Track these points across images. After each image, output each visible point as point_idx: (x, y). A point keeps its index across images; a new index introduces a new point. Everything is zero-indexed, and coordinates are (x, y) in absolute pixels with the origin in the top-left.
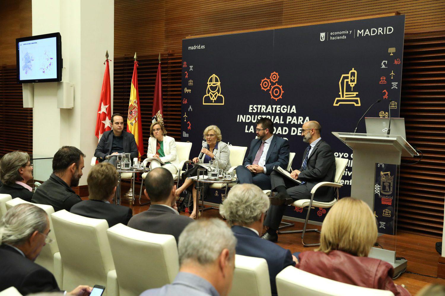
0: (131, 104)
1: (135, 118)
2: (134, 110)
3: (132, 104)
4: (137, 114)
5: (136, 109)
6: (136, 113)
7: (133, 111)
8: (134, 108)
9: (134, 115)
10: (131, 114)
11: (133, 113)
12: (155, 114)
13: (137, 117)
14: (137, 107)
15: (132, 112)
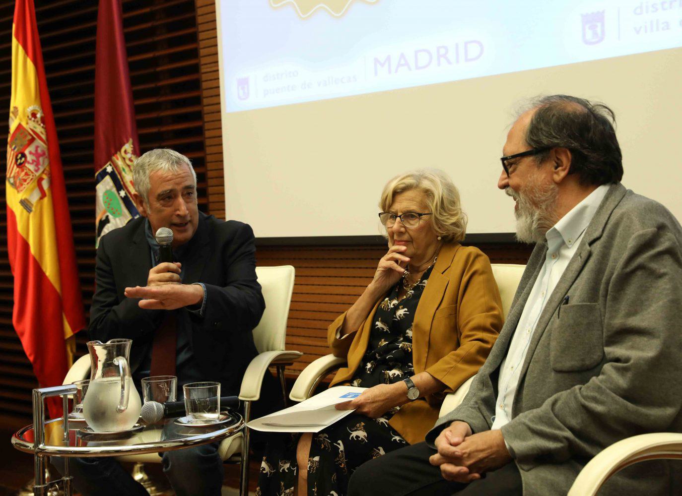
0: (20, 126)
1: (40, 180)
2: (32, 148)
3: (24, 124)
4: (44, 163)
5: (38, 142)
6: (41, 159)
7: (27, 152)
8: (33, 140)
9: (31, 167)
10: (21, 166)
11: (30, 158)
12: (109, 158)
13: (45, 176)
14: (44, 137)
15: (24, 155)
